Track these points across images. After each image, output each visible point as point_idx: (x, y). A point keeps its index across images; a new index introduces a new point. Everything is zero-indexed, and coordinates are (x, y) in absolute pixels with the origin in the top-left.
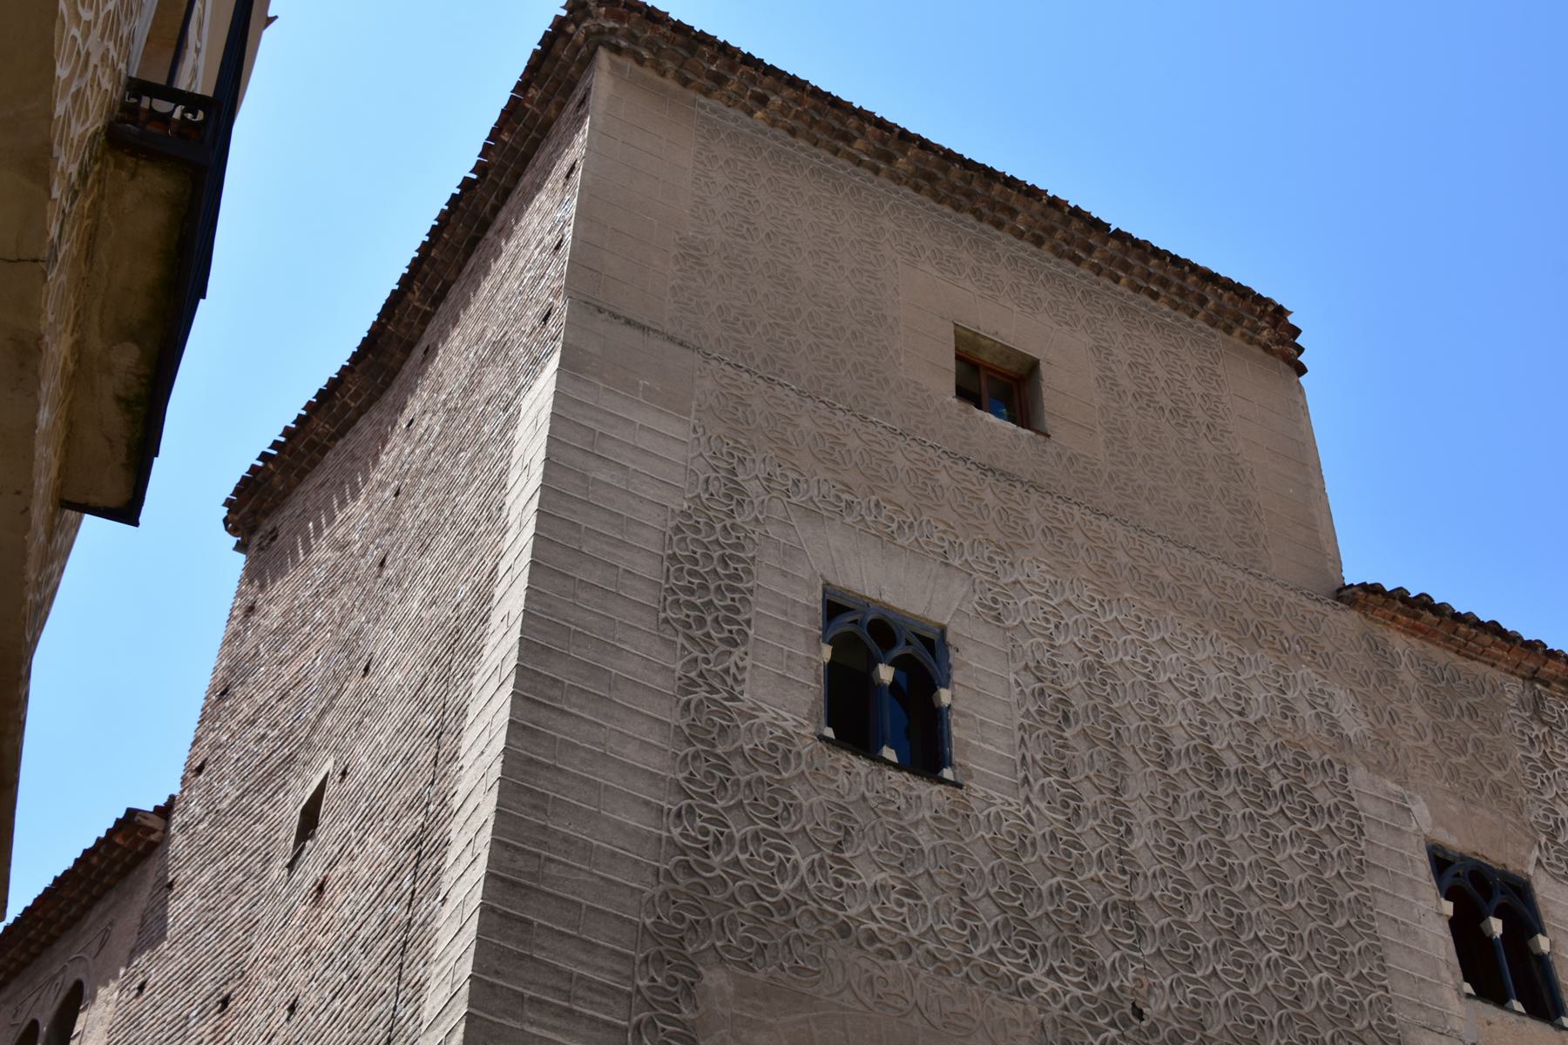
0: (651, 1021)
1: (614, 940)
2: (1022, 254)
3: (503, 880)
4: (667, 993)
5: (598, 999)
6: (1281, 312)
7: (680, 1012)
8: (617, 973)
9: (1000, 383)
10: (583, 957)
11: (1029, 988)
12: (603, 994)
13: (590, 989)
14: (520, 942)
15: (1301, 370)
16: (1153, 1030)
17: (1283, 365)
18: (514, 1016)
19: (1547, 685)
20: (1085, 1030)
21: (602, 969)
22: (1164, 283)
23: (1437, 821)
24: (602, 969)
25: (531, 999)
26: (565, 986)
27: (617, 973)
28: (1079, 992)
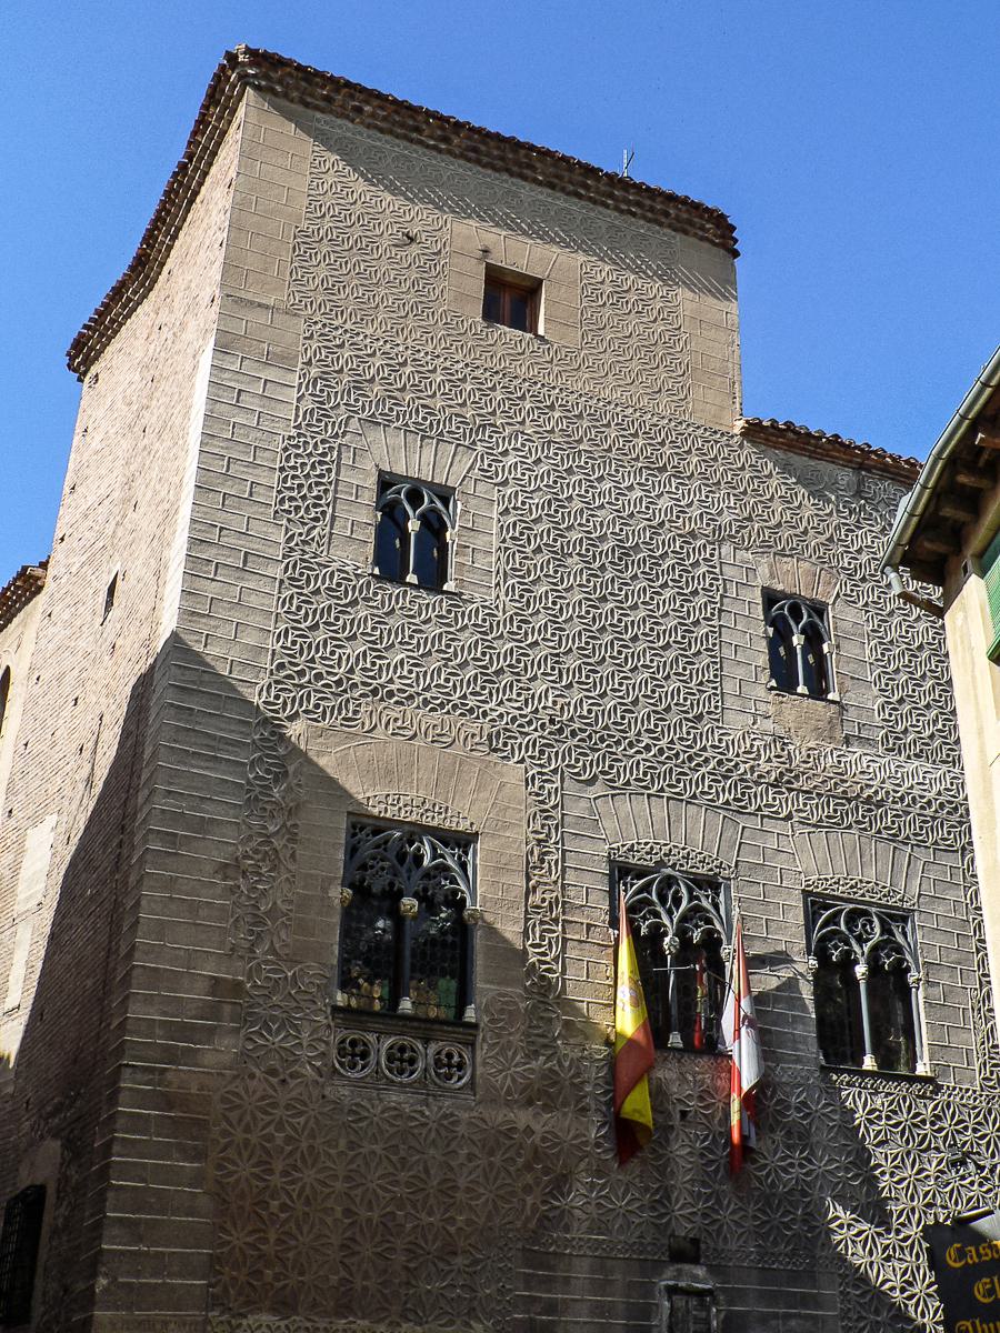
0: (260, 758)
1: (240, 714)
2: (540, 197)
3: (177, 686)
4: (270, 741)
5: (230, 748)
6: (723, 217)
7: (277, 751)
8: (241, 733)
9: (512, 299)
10: (223, 726)
11: (485, 714)
12: (233, 745)
13: (226, 744)
14: (187, 722)
15: (736, 254)
16: (560, 731)
17: (722, 252)
18: (185, 764)
19: (869, 471)
20: (517, 735)
21: (233, 731)
22: (638, 204)
23: (772, 576)
24: (233, 731)
25: (194, 753)
26: (213, 743)
27: (241, 733)
28: (517, 712)
